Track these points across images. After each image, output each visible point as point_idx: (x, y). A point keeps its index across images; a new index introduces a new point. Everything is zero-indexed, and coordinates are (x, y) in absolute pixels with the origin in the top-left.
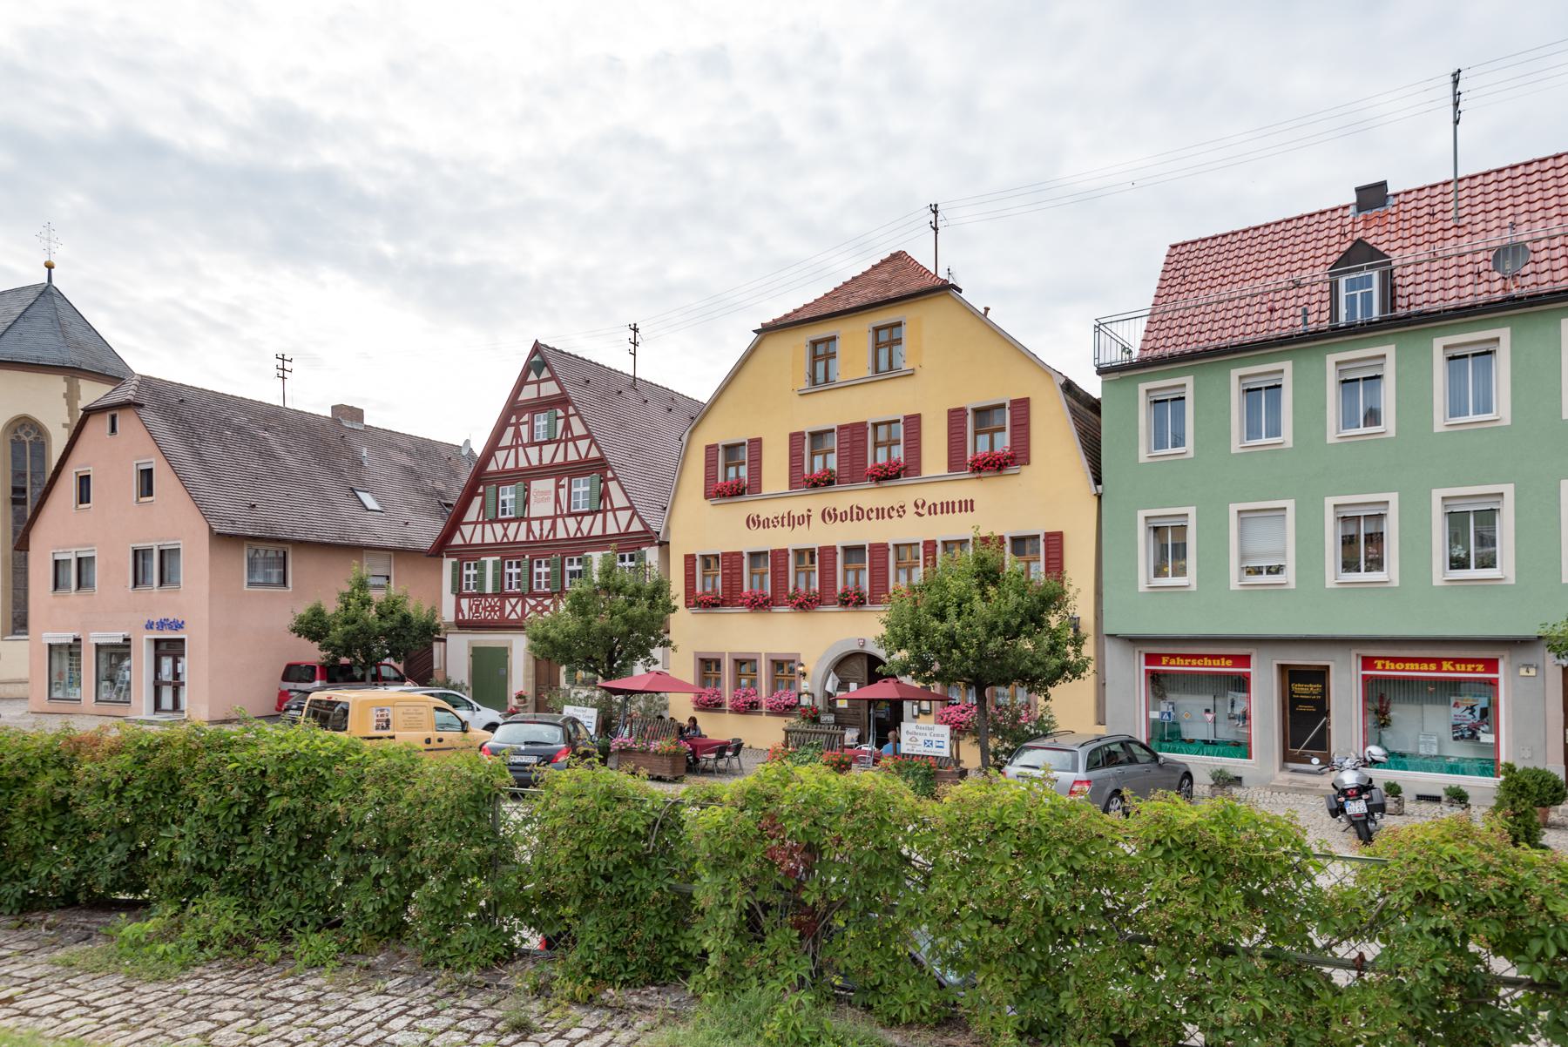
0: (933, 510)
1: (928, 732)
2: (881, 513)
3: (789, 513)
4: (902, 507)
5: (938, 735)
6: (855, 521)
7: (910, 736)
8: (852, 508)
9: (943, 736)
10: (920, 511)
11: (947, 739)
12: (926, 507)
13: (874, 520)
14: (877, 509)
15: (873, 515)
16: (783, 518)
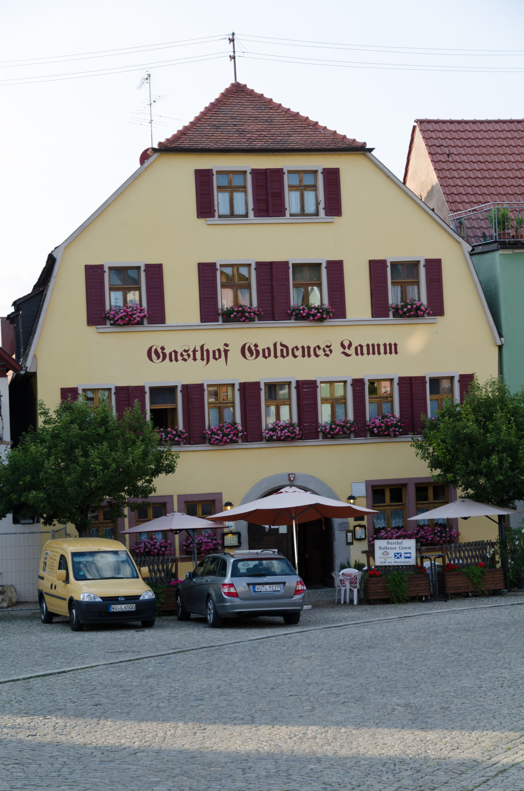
0: (359, 350)
1: (397, 546)
2: (306, 352)
3: (202, 347)
4: (327, 346)
5: (406, 548)
6: (280, 358)
7: (382, 551)
8: (275, 345)
9: (410, 548)
10: (347, 351)
11: (413, 551)
12: (353, 348)
13: (300, 357)
14: (303, 348)
15: (299, 353)
16: (194, 351)
